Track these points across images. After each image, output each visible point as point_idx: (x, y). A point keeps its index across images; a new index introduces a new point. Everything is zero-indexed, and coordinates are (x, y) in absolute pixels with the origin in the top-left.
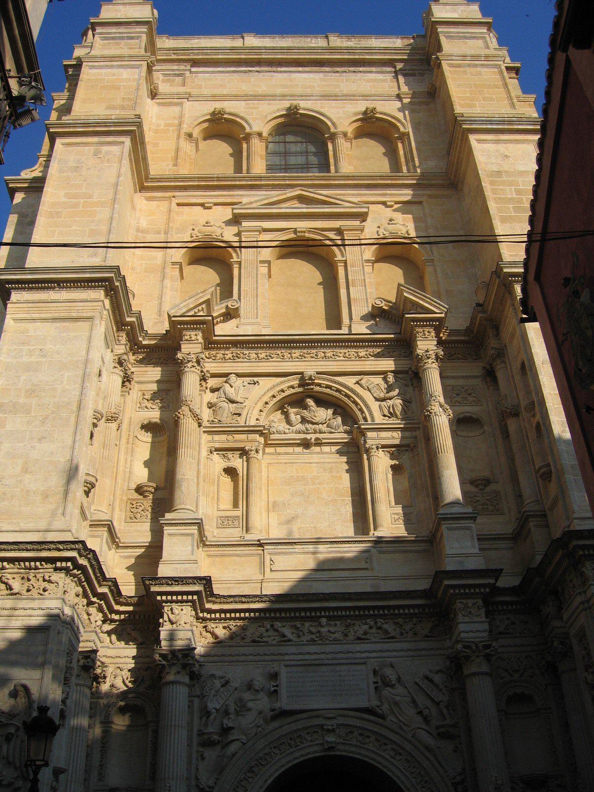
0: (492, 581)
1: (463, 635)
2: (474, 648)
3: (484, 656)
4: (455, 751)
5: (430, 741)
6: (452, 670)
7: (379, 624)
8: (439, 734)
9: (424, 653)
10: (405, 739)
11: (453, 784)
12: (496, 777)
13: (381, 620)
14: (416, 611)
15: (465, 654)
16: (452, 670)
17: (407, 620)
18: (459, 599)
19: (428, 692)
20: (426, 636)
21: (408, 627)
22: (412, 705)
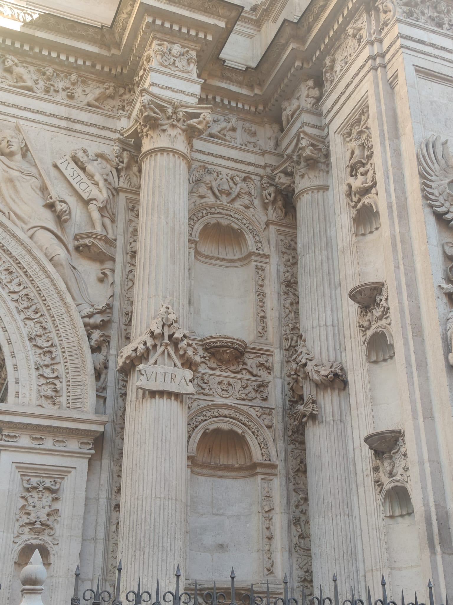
0: (222, 24)
1: (155, 90)
2: (170, 111)
3: (184, 131)
4: (101, 281)
5: (60, 252)
6: (122, 162)
7: (9, 63)
8: (77, 248)
9: (78, 127)
10: (14, 236)
11: (86, 325)
12: (167, 308)
13: (16, 61)
14: (80, 62)
15: (153, 115)
16: (122, 162)
17: (62, 75)
18: (159, 39)
19: (73, 183)
20: (89, 105)
21: (60, 85)
22: (40, 193)
